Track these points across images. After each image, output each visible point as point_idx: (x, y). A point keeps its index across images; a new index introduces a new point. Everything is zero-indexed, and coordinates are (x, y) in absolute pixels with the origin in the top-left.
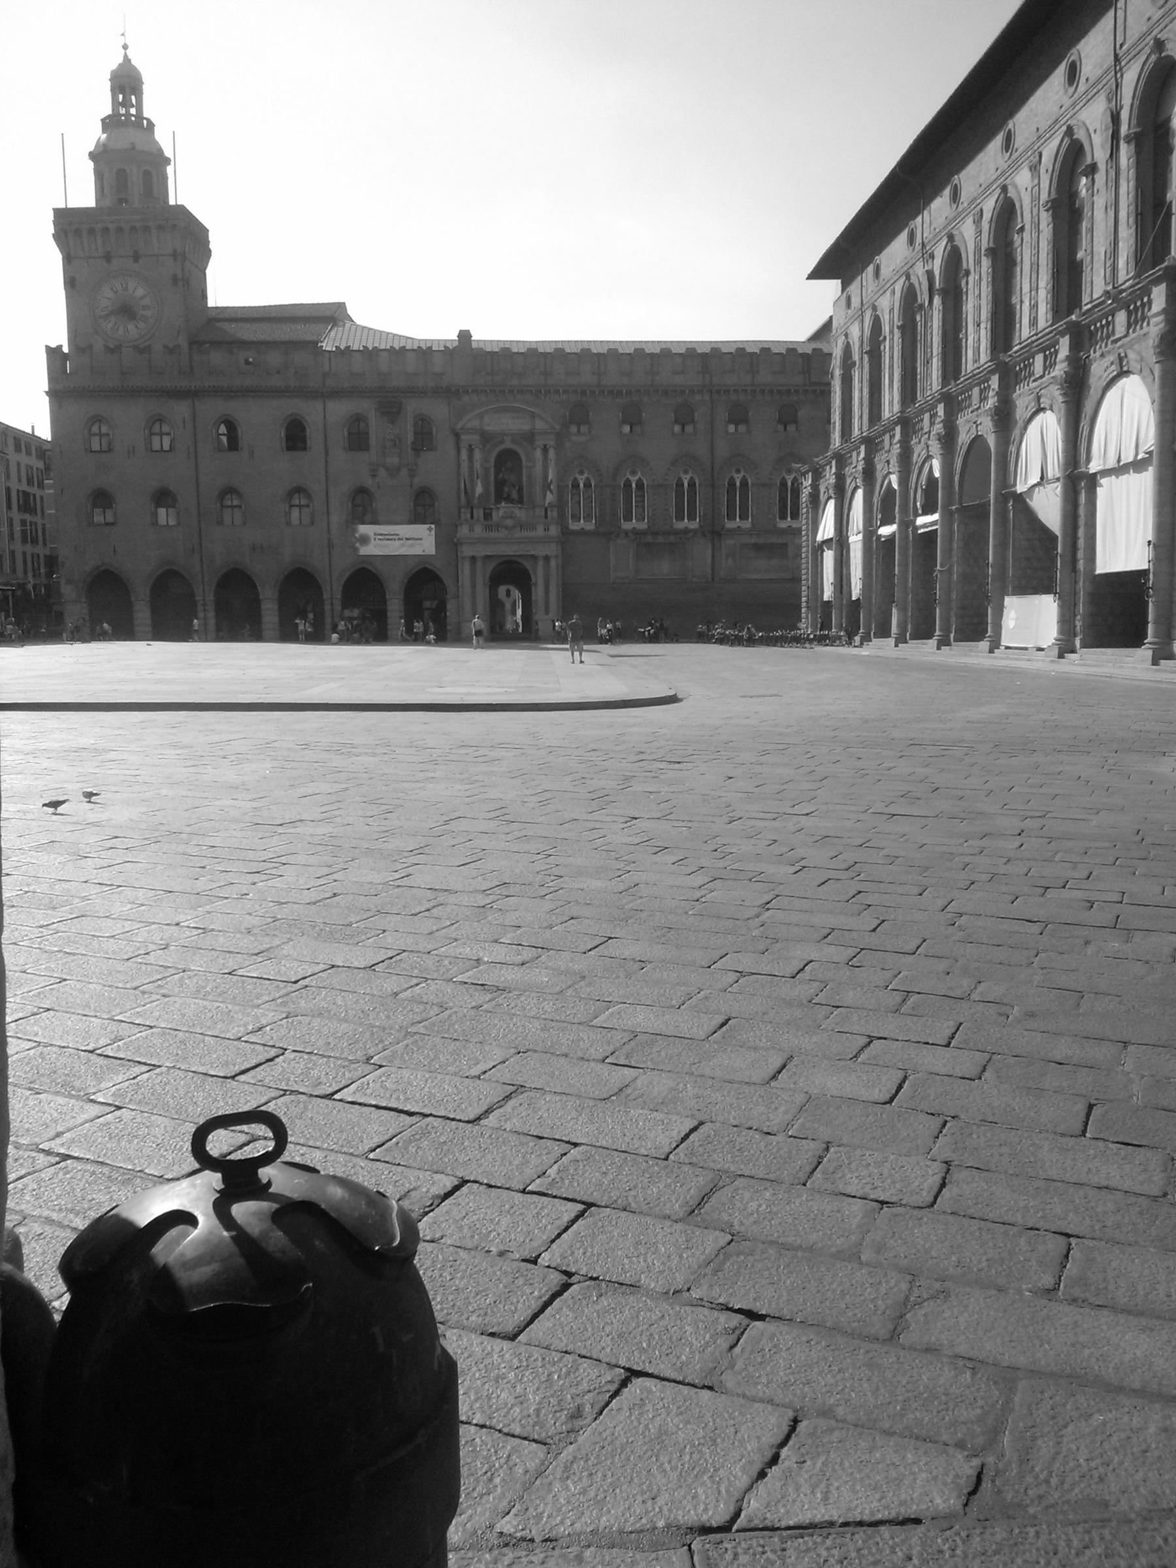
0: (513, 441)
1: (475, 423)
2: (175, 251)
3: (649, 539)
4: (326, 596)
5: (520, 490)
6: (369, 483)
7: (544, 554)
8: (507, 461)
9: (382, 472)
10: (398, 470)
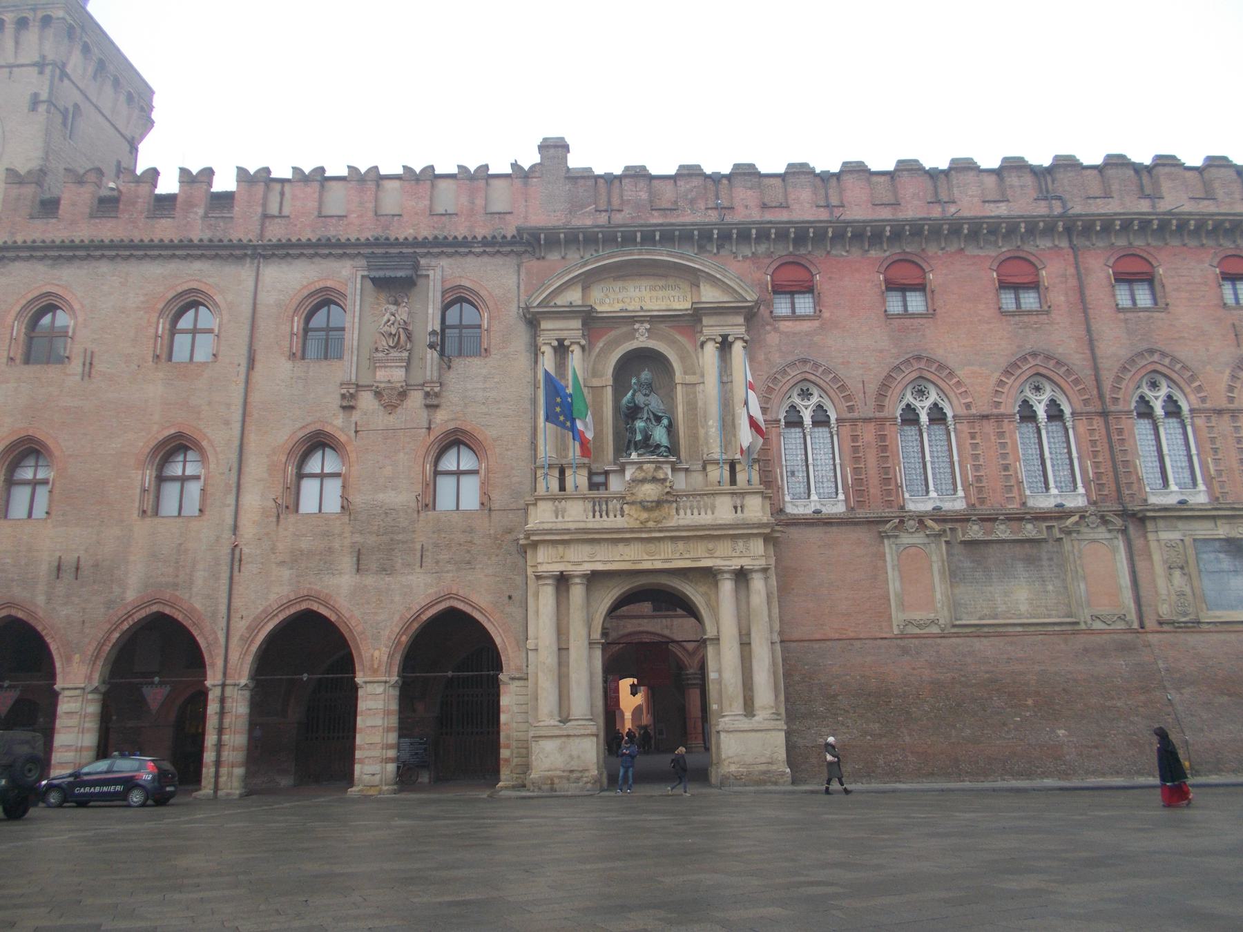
1: (574, 296)
2: (44, 57)
3: (975, 532)
4: (213, 679)
5: (671, 429)
6: (337, 424)
7: (736, 564)
8: (642, 366)
9: (366, 401)
10: (403, 395)
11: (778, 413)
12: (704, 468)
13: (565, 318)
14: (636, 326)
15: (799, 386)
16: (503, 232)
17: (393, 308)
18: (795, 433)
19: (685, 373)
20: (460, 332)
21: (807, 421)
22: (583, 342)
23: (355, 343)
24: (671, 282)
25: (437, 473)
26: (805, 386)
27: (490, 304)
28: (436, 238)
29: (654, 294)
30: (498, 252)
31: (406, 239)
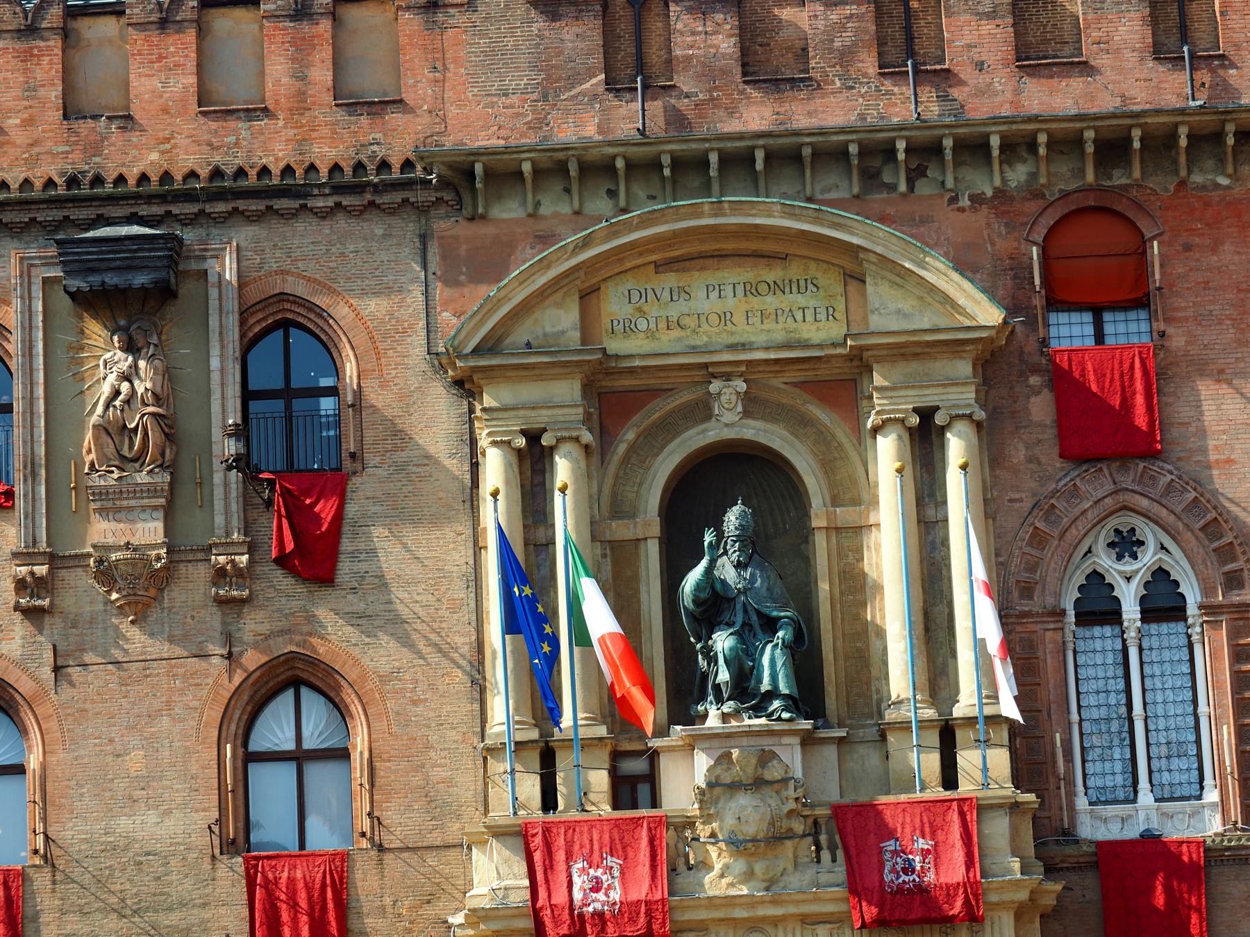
0: (752, 405)
1: (562, 320)
11: (1058, 595)
12: (883, 737)
13: (540, 378)
14: (715, 386)
15: (1113, 522)
16: (381, 152)
17: (124, 361)
18: (1102, 637)
19: (836, 501)
20: (288, 407)
21: (1131, 611)
22: (587, 437)
23: (42, 451)
24: (794, 271)
25: (250, 758)
26: (1124, 521)
27: (361, 339)
28: (217, 173)
29: (756, 302)
30: (372, 204)
31: (144, 178)
